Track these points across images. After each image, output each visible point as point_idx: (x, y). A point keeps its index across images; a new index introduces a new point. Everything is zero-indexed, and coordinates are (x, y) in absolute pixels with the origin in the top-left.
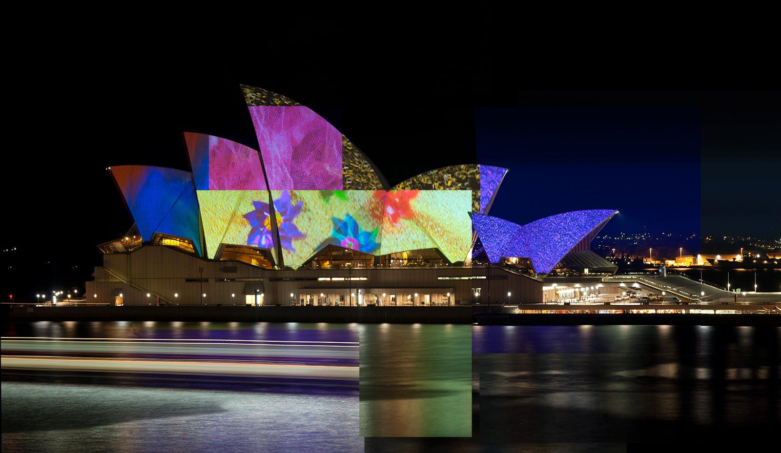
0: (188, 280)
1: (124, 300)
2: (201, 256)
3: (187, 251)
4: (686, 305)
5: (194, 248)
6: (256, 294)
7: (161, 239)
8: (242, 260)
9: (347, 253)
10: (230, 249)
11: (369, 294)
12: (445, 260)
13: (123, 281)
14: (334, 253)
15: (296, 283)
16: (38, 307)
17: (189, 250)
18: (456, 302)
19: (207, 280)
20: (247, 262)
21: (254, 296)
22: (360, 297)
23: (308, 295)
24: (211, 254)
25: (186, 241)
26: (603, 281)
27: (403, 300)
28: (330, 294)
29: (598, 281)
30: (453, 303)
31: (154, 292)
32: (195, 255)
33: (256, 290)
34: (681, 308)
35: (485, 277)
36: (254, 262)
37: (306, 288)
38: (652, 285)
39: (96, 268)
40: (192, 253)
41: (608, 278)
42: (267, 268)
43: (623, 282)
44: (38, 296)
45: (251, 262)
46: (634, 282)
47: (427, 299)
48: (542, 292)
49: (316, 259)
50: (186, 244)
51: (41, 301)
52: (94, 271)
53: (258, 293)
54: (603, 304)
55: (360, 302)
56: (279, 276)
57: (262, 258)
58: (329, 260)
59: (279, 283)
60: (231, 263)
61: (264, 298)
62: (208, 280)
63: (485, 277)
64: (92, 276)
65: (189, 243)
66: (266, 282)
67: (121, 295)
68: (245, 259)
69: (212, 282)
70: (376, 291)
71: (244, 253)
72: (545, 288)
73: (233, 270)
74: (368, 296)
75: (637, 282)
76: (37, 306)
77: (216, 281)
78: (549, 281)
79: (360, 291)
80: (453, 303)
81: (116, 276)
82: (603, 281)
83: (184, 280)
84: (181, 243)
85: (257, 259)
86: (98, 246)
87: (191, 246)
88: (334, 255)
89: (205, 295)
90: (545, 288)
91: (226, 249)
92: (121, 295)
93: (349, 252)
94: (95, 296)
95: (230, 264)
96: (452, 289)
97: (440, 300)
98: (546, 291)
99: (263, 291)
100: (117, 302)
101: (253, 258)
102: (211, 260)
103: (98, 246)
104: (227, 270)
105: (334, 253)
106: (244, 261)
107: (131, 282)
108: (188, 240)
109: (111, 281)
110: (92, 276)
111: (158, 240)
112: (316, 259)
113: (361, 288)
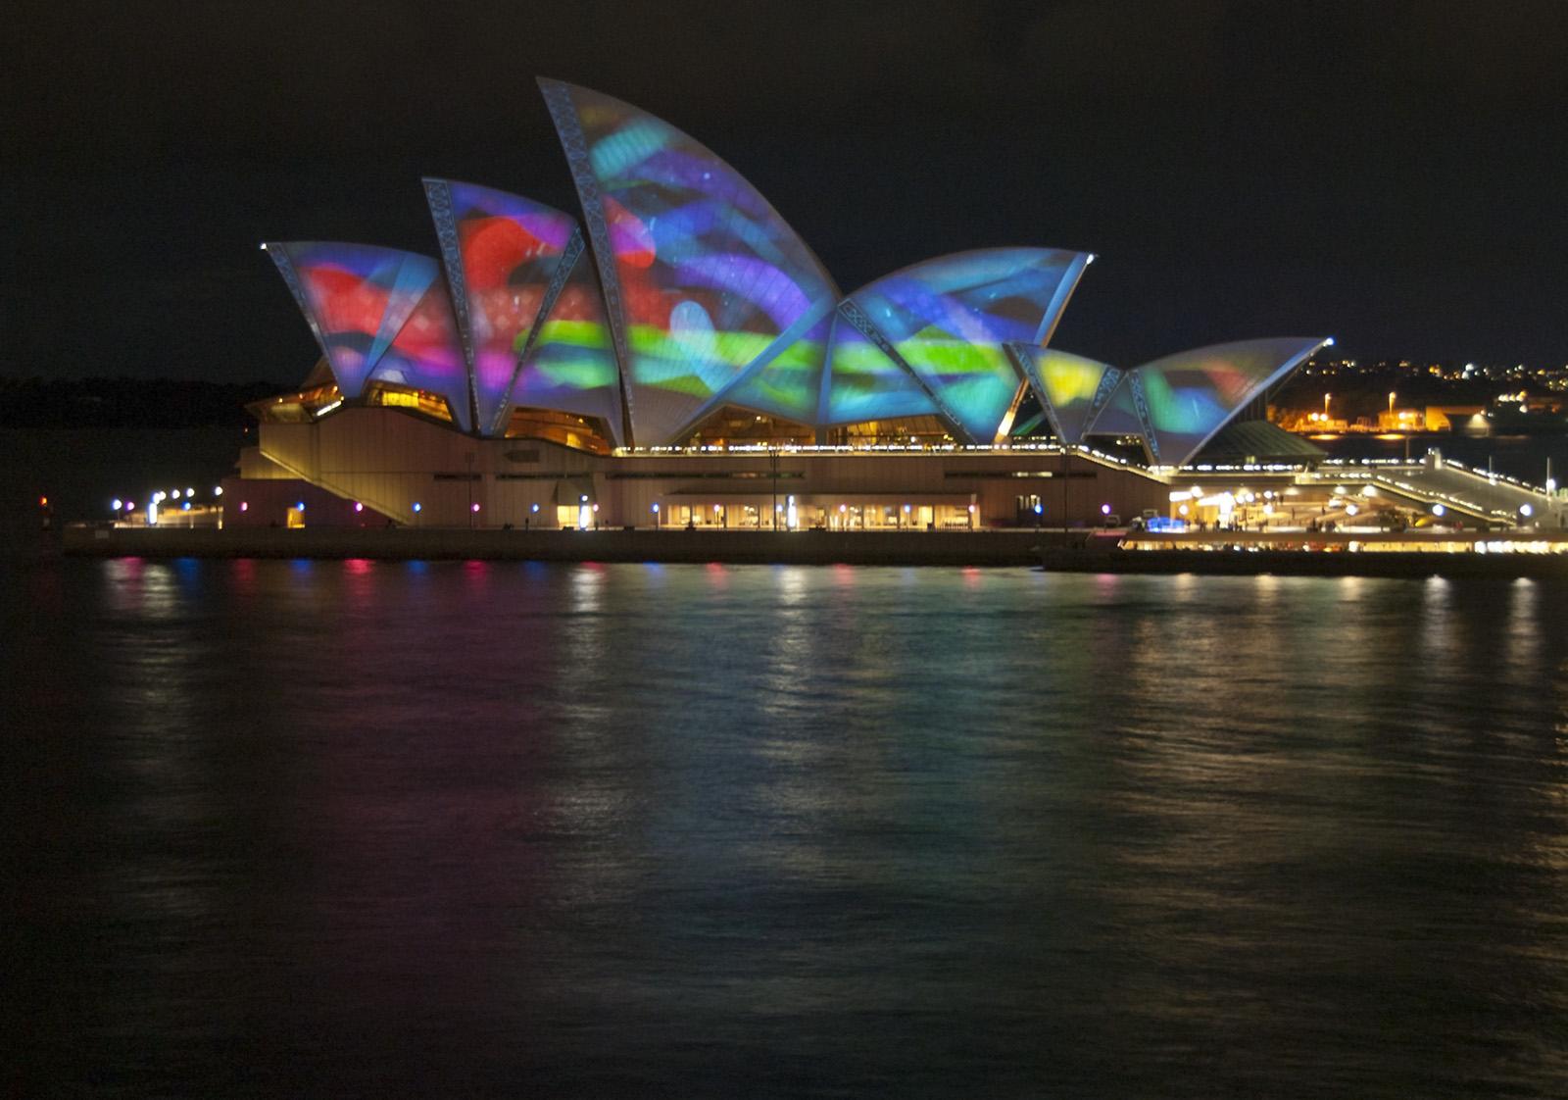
0: (439, 477)
1: (306, 517)
2: (466, 426)
4: (1484, 531)
5: (451, 410)
6: (581, 503)
7: (381, 394)
8: (548, 437)
9: (760, 424)
10: (526, 416)
11: (809, 507)
13: (303, 477)
15: (659, 483)
16: (118, 529)
18: (983, 519)
19: (477, 477)
20: (559, 440)
21: (575, 509)
22: (793, 511)
23: (685, 505)
24: (486, 424)
25: (434, 398)
26: (1297, 482)
27: (876, 518)
28: (729, 504)
29: (1287, 482)
30: (976, 525)
31: (369, 500)
32: (451, 426)
33: (580, 498)
34: (1473, 538)
35: (1049, 474)
36: (572, 441)
37: (680, 492)
38: (1403, 489)
39: (243, 453)
41: (1304, 477)
42: (600, 453)
44: (117, 505)
45: (566, 440)
46: (1365, 485)
47: (925, 516)
48: (1168, 503)
50: (432, 404)
51: (123, 514)
52: (237, 458)
53: (585, 503)
54: (1304, 529)
55: (792, 524)
56: (625, 469)
57: (590, 432)
58: (725, 437)
59: (626, 482)
60: (528, 442)
62: (477, 477)
63: (1049, 474)
64: (237, 466)
65: (438, 402)
66: (599, 479)
67: (302, 507)
68: (553, 435)
69: (489, 480)
70: (823, 499)
71: (554, 423)
72: (1175, 497)
73: (533, 456)
74: (806, 510)
75: (1372, 485)
76: (117, 526)
77: (497, 478)
78: (1182, 482)
79: (792, 499)
80: (976, 525)
81: (287, 467)
82: (1297, 482)
83: (433, 478)
84: (423, 401)
85: (579, 436)
86: (246, 406)
87: (444, 407)
88: (735, 428)
89: (476, 508)
90: (1175, 497)
91: (518, 415)
92: (302, 507)
93: (764, 421)
94: (245, 507)
95: (525, 446)
96: (974, 497)
97: (952, 518)
98: (1176, 503)
99: (592, 501)
100: (290, 518)
101: (566, 432)
103: (246, 406)
104: (512, 456)
106: (554, 439)
107: (320, 480)
108: (437, 396)
109: (276, 476)
110: (237, 466)
111: (374, 396)
112: (698, 435)
113: (792, 493)
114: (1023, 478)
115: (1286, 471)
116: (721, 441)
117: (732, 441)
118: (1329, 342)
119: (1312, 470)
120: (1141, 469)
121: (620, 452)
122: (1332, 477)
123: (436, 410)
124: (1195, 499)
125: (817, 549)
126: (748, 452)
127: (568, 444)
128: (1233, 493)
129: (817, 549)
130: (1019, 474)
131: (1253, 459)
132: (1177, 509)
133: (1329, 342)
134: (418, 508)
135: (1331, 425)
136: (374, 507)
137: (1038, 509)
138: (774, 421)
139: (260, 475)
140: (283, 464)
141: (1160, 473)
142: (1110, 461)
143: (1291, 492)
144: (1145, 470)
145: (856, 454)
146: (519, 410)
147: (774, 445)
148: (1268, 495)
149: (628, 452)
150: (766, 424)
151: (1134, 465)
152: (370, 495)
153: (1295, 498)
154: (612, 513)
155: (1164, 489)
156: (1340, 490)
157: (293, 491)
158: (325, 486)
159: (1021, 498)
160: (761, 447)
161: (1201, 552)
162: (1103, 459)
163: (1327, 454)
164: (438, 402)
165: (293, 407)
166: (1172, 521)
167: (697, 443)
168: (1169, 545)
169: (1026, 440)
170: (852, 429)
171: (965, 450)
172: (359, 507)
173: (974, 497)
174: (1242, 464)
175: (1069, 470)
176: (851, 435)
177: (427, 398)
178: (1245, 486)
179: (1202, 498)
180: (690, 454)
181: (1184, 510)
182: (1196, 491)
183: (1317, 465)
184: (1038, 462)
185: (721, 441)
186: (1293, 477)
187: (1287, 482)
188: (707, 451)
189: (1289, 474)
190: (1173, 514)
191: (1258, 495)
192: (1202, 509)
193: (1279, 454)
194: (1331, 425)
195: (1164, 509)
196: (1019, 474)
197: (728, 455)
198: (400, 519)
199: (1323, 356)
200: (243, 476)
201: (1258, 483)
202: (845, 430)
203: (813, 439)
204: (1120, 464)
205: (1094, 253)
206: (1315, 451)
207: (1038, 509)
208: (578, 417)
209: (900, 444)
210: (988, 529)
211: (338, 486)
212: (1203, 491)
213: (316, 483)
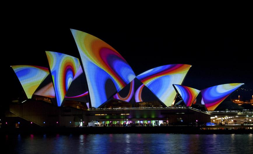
1: (19, 125)
3: (48, 103)
12: (164, 106)
14: (114, 103)
17: (49, 102)
26: (238, 114)
29: (236, 114)
35: (184, 113)
36: (78, 107)
40: (50, 103)
41: (239, 113)
43: (248, 115)
49: (106, 106)
50: (47, 100)
57: (82, 105)
61: (83, 123)
63: (184, 113)
65: (49, 99)
68: (74, 106)
72: (211, 118)
78: (213, 115)
79: (127, 120)
82: (238, 114)
85: (79, 106)
87: (50, 100)
92: (19, 123)
99: (82, 121)
101: (77, 105)
102: (59, 107)
105: (114, 103)
106: (74, 107)
109: (13, 116)
112: (106, 106)
114: (178, 114)
115: (236, 112)
116: (111, 107)
117: (113, 107)
118: (244, 84)
119: (241, 112)
120: (204, 112)
121: (88, 110)
122: (246, 113)
123: (48, 101)
124: (216, 118)
125: (133, 129)
126: (117, 109)
127: (78, 108)
128: (223, 117)
129: (133, 129)
130: (177, 113)
131: (228, 110)
132: (213, 121)
133: (244, 84)
134: (44, 123)
135: (240, 102)
136: (35, 123)
137: (182, 121)
138: (122, 102)
139: (9, 116)
140: (15, 114)
141: (208, 113)
142: (197, 110)
143: (237, 116)
144: (205, 112)
145: (141, 109)
146: (66, 101)
147: (123, 108)
148: (231, 117)
149: (90, 110)
150: (121, 103)
151: (202, 111)
152: (33, 120)
153: (237, 118)
154: (85, 125)
155: (209, 116)
156: (247, 116)
157: (17, 119)
158: (23, 118)
159: (178, 119)
160: (120, 108)
161: (218, 130)
162: (196, 110)
163: (244, 108)
164: (49, 99)
165: (17, 101)
166: (211, 123)
167: (106, 107)
168: (211, 129)
169: (177, 106)
170: (140, 104)
171: (165, 108)
172: (32, 123)
173: (167, 118)
174: (226, 111)
175: (188, 111)
176: (140, 105)
177: (46, 99)
178: (227, 115)
179: (217, 118)
180: (104, 110)
181: (214, 121)
182: (216, 117)
183: (242, 111)
184: (181, 111)
185: (111, 107)
186: (237, 113)
187: (236, 114)
188: (108, 109)
189: (236, 113)
190: (211, 121)
191: (229, 117)
192: (218, 120)
193: (234, 108)
194: (240, 102)
195: (209, 121)
196: (177, 113)
197: (113, 110)
198: (40, 125)
199: (242, 86)
200: (6, 116)
201: (229, 115)
202: (138, 104)
203: (131, 106)
204: (199, 111)
205: (192, 65)
206: (241, 108)
207: (182, 121)
208: (79, 102)
209: (150, 107)
210: (171, 126)
211: (26, 118)
212: (218, 117)
213: (22, 118)
